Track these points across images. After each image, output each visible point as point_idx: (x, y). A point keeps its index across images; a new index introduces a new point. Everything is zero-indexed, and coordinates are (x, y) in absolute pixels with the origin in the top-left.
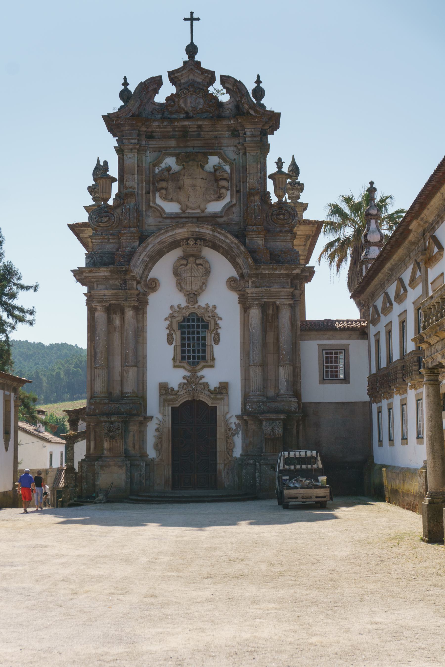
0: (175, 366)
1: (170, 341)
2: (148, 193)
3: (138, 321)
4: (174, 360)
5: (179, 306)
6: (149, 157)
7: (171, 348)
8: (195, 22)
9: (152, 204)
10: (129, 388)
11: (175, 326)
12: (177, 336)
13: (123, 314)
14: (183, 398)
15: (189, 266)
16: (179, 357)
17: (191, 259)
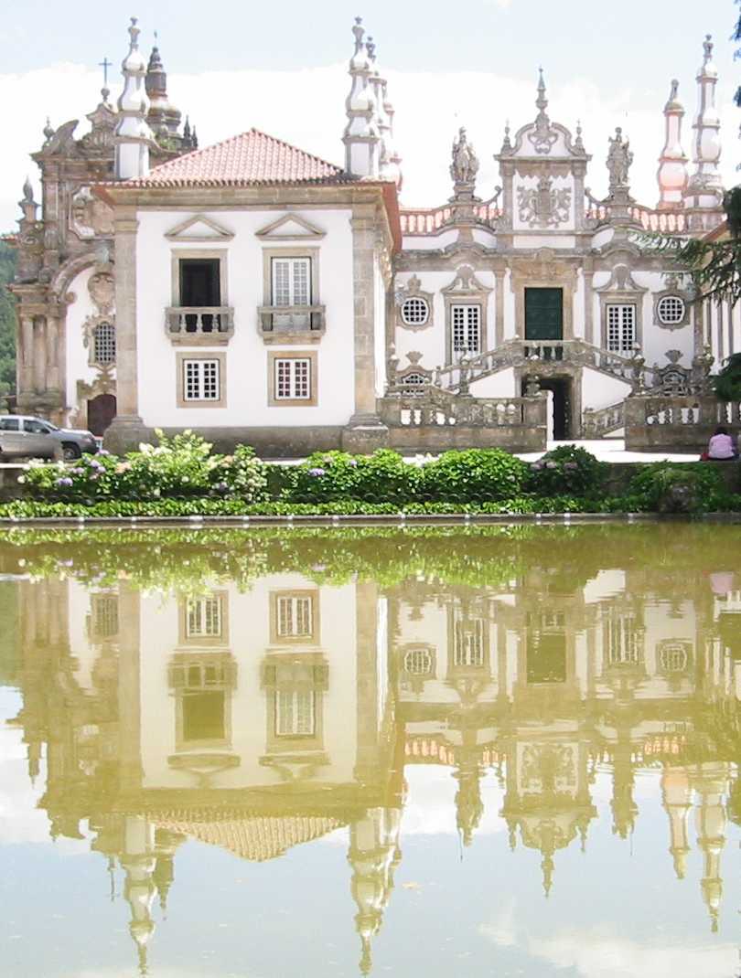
0: (90, 366)
1: (86, 346)
2: (67, 218)
3: (58, 329)
4: (89, 361)
5: (93, 317)
6: (67, 188)
7: (87, 351)
8: (108, 67)
9: (70, 228)
10: (52, 384)
11: (90, 334)
12: (92, 341)
13: (46, 320)
14: (97, 393)
15: (101, 282)
16: (93, 358)
17: (102, 277)
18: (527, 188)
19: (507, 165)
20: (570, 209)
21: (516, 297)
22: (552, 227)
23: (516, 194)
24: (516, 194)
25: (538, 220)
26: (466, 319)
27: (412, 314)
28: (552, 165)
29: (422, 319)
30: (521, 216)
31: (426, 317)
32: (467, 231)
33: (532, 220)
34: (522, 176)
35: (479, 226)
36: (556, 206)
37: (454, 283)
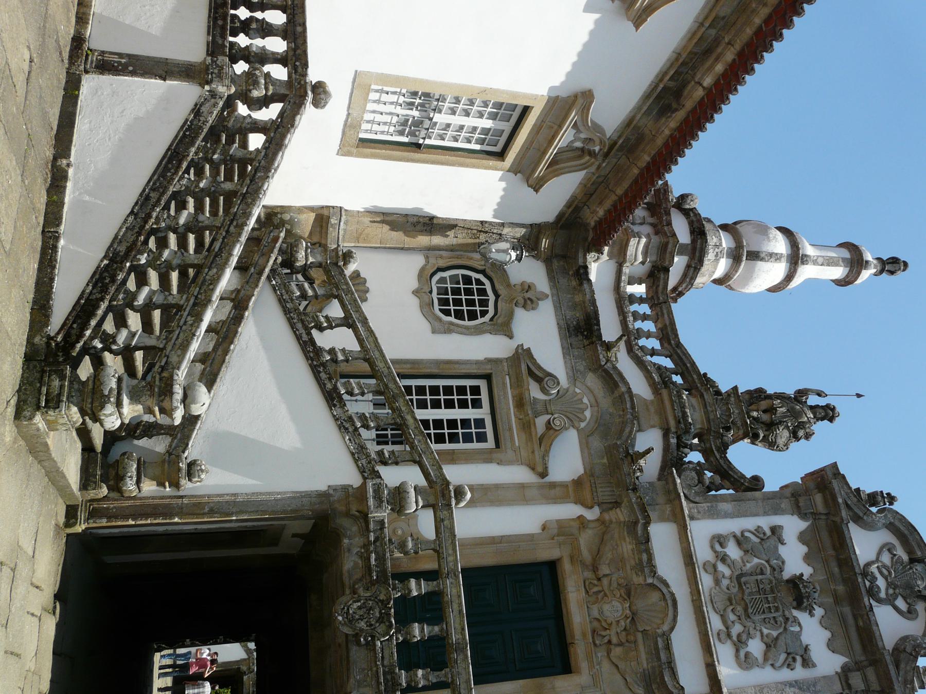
18: (783, 550)
19: (818, 498)
20: (768, 669)
21: (530, 537)
22: (715, 623)
23: (765, 522)
24: (765, 522)
25: (725, 582)
26: (457, 414)
27: (456, 291)
28: (847, 610)
29: (447, 313)
30: (719, 540)
31: (452, 319)
32: (655, 419)
33: (721, 568)
34: (803, 538)
35: (673, 441)
36: (766, 631)
37: (541, 377)
